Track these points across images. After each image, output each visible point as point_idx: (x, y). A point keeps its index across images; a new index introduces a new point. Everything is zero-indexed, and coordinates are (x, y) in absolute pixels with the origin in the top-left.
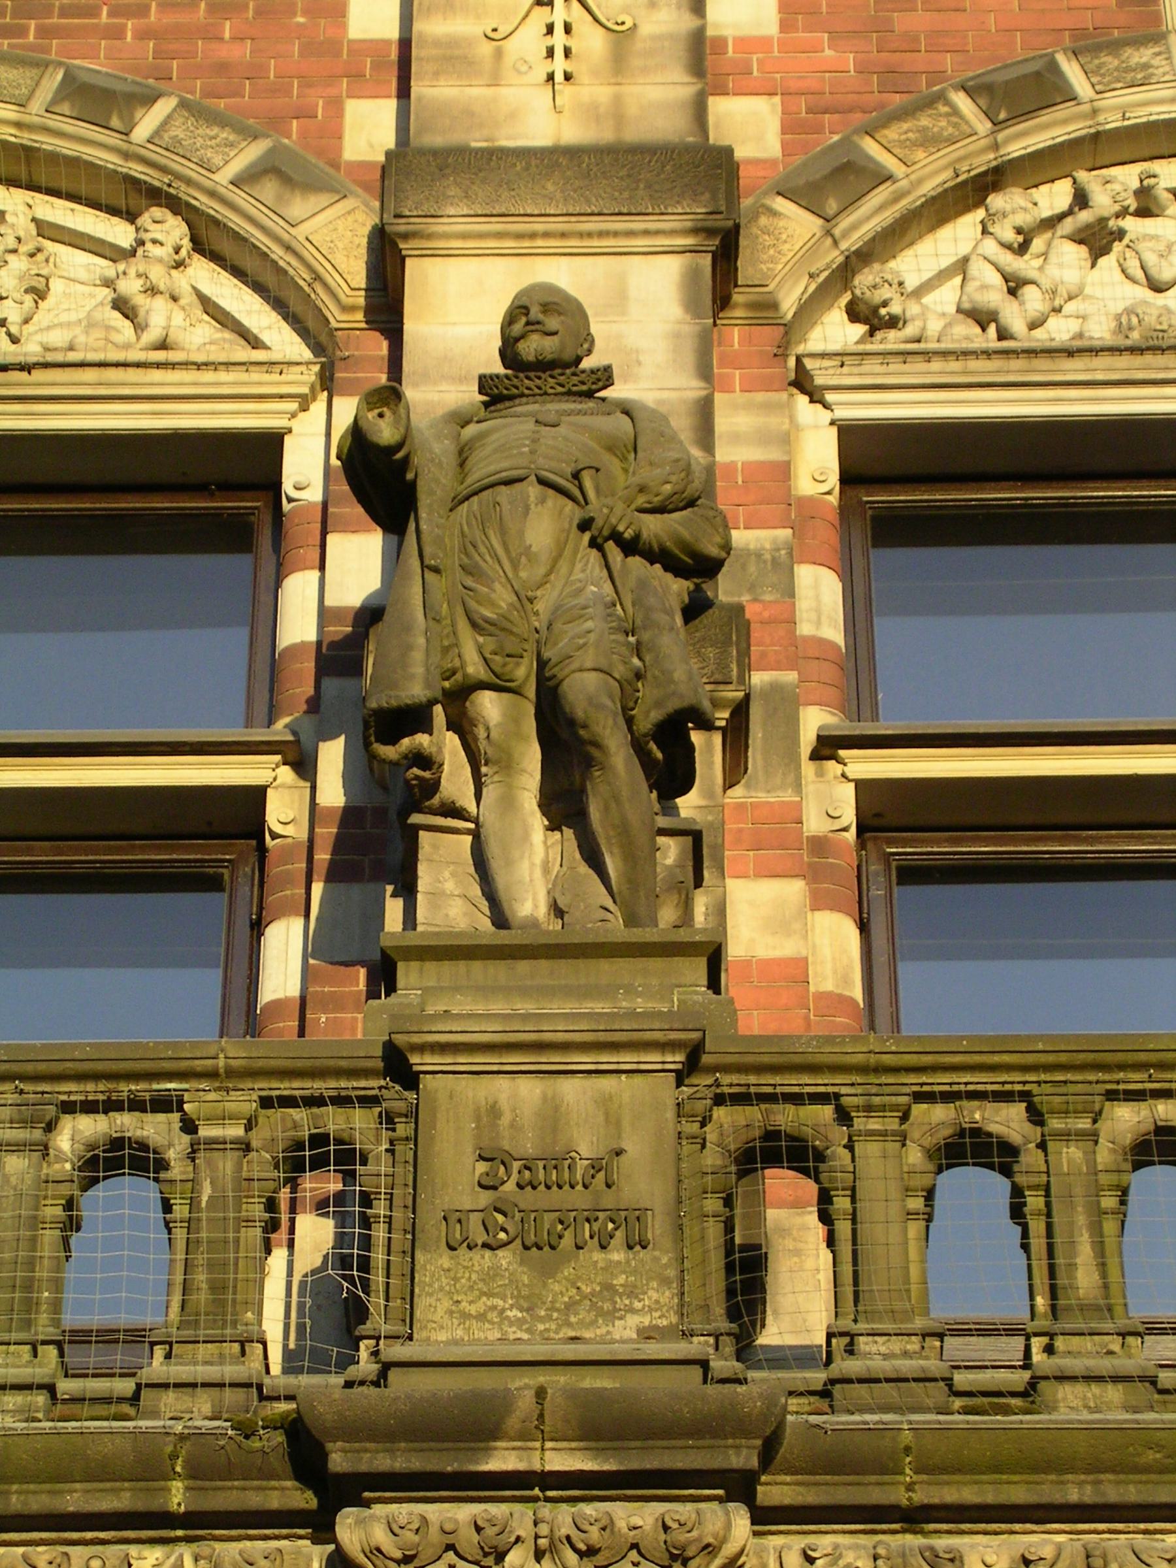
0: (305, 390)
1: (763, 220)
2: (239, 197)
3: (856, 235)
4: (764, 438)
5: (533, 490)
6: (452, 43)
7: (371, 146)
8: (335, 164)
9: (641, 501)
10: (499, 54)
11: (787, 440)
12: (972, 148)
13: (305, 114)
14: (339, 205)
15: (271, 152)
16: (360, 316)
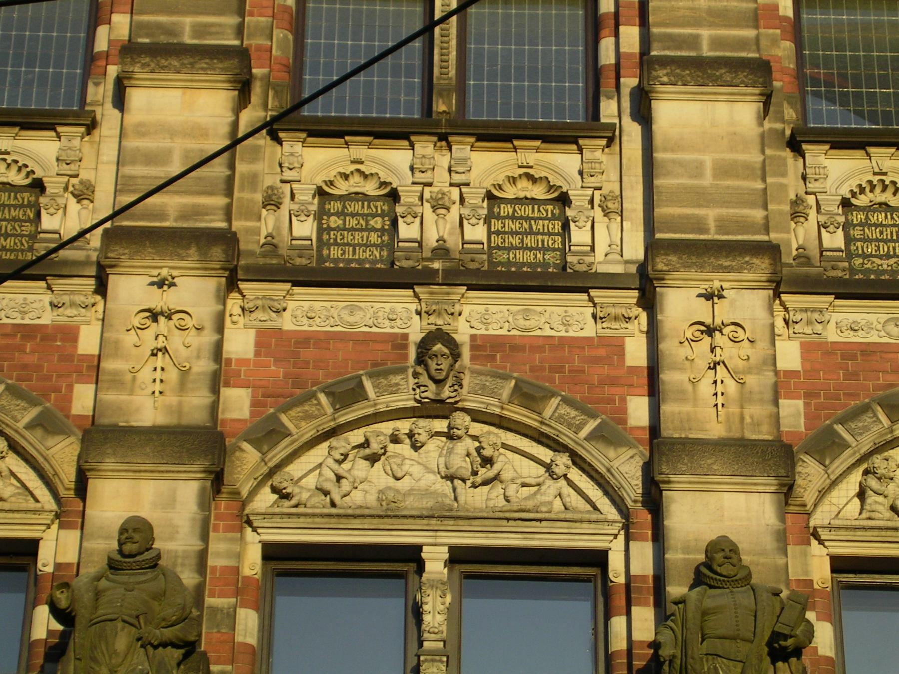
0: (49, 522)
1: (238, 454)
2: (27, 434)
3: (274, 460)
4: (229, 555)
5: (120, 624)
6: (116, 373)
7: (83, 408)
8: (68, 417)
9: (163, 624)
10: (134, 379)
11: (239, 556)
12: (324, 421)
13: (57, 390)
14: (67, 440)
15: (41, 414)
16: (72, 492)
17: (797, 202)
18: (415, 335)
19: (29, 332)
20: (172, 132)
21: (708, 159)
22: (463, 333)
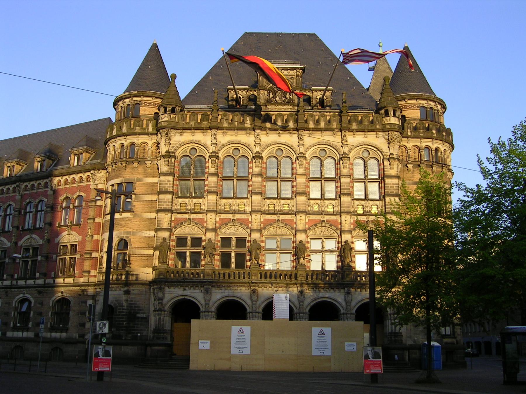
17: (264, 205)
18: (232, 219)
19: (200, 218)
20: (211, 200)
21: (256, 202)
22: (236, 219)
